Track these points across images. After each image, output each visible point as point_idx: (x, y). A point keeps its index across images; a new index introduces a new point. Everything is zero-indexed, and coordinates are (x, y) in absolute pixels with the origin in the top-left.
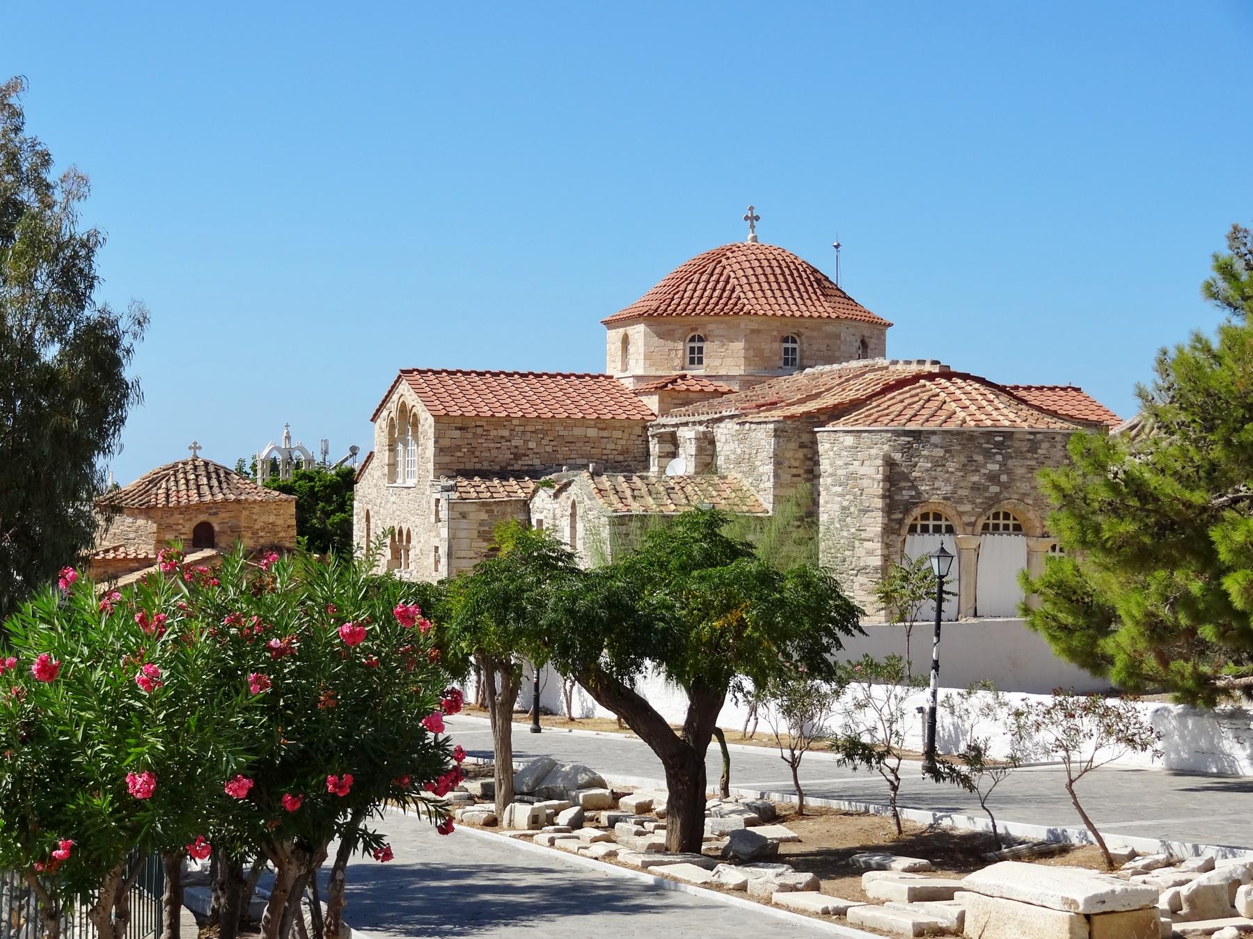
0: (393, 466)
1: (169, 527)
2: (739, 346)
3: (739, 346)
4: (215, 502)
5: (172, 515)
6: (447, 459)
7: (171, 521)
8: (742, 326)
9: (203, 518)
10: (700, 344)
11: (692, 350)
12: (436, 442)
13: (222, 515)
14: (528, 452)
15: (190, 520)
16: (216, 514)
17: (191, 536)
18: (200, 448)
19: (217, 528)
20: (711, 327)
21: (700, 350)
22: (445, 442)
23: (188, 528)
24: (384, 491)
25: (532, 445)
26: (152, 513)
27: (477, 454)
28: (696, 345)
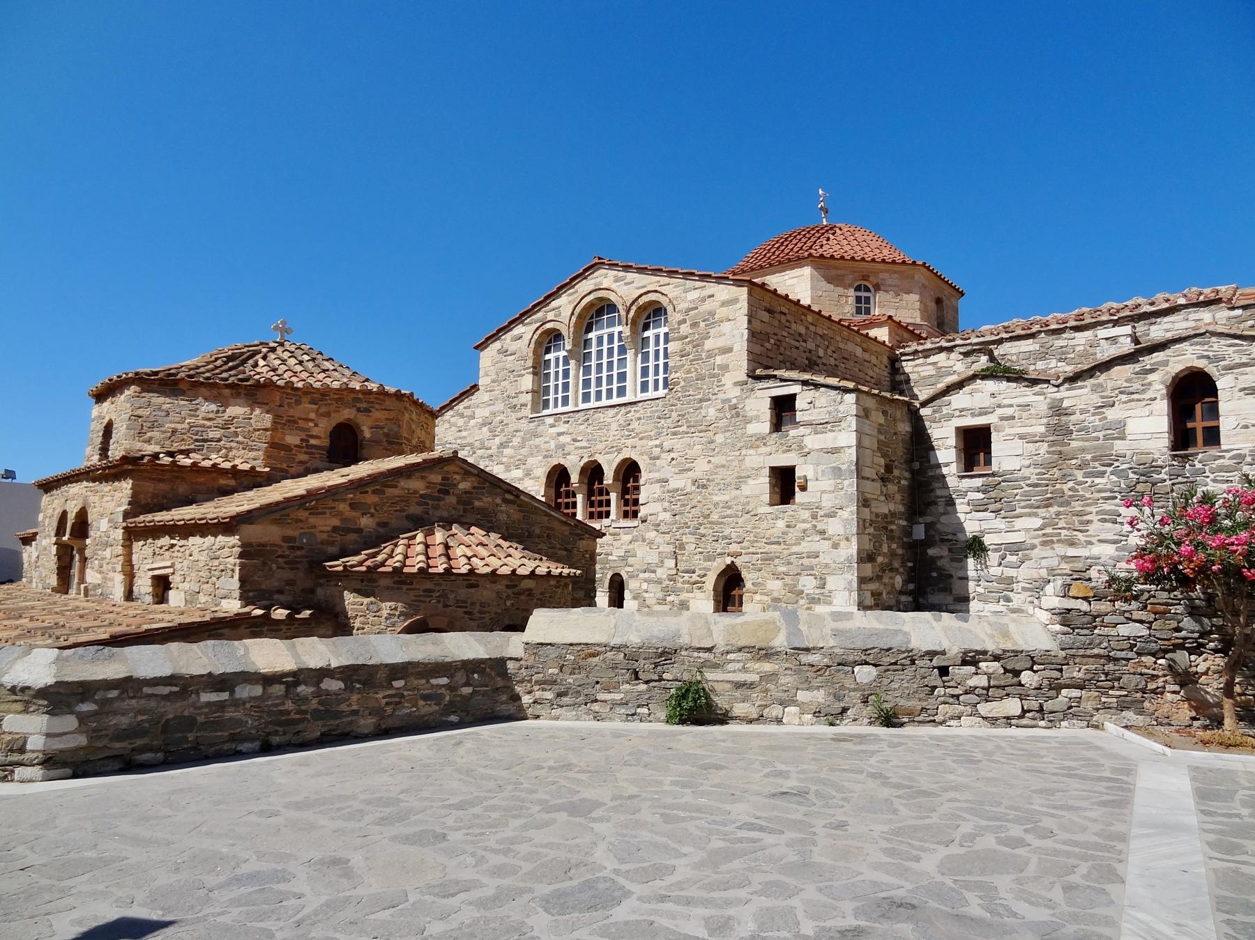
0: (540, 397)
1: (292, 422)
2: (914, 298)
3: (914, 298)
4: (370, 392)
5: (298, 402)
6: (758, 349)
7: (297, 412)
8: (916, 277)
9: (347, 414)
10: (867, 294)
11: (858, 300)
12: (749, 322)
13: (377, 414)
14: (819, 361)
15: (328, 414)
16: (367, 411)
17: (326, 442)
18: (288, 331)
19: (367, 434)
20: (882, 276)
21: (867, 300)
22: (757, 325)
23: (321, 430)
24: (523, 425)
25: (821, 353)
26: (260, 395)
27: (782, 349)
28: (863, 294)
